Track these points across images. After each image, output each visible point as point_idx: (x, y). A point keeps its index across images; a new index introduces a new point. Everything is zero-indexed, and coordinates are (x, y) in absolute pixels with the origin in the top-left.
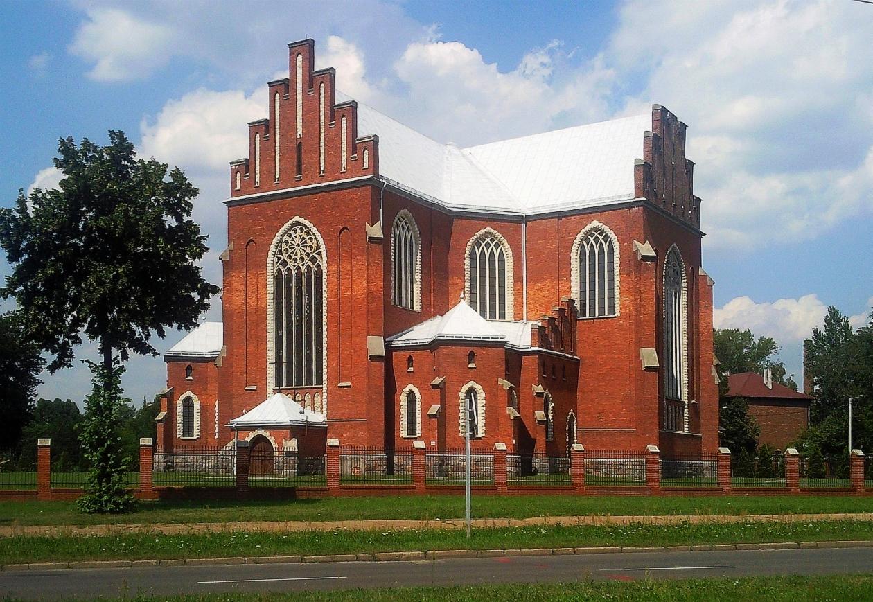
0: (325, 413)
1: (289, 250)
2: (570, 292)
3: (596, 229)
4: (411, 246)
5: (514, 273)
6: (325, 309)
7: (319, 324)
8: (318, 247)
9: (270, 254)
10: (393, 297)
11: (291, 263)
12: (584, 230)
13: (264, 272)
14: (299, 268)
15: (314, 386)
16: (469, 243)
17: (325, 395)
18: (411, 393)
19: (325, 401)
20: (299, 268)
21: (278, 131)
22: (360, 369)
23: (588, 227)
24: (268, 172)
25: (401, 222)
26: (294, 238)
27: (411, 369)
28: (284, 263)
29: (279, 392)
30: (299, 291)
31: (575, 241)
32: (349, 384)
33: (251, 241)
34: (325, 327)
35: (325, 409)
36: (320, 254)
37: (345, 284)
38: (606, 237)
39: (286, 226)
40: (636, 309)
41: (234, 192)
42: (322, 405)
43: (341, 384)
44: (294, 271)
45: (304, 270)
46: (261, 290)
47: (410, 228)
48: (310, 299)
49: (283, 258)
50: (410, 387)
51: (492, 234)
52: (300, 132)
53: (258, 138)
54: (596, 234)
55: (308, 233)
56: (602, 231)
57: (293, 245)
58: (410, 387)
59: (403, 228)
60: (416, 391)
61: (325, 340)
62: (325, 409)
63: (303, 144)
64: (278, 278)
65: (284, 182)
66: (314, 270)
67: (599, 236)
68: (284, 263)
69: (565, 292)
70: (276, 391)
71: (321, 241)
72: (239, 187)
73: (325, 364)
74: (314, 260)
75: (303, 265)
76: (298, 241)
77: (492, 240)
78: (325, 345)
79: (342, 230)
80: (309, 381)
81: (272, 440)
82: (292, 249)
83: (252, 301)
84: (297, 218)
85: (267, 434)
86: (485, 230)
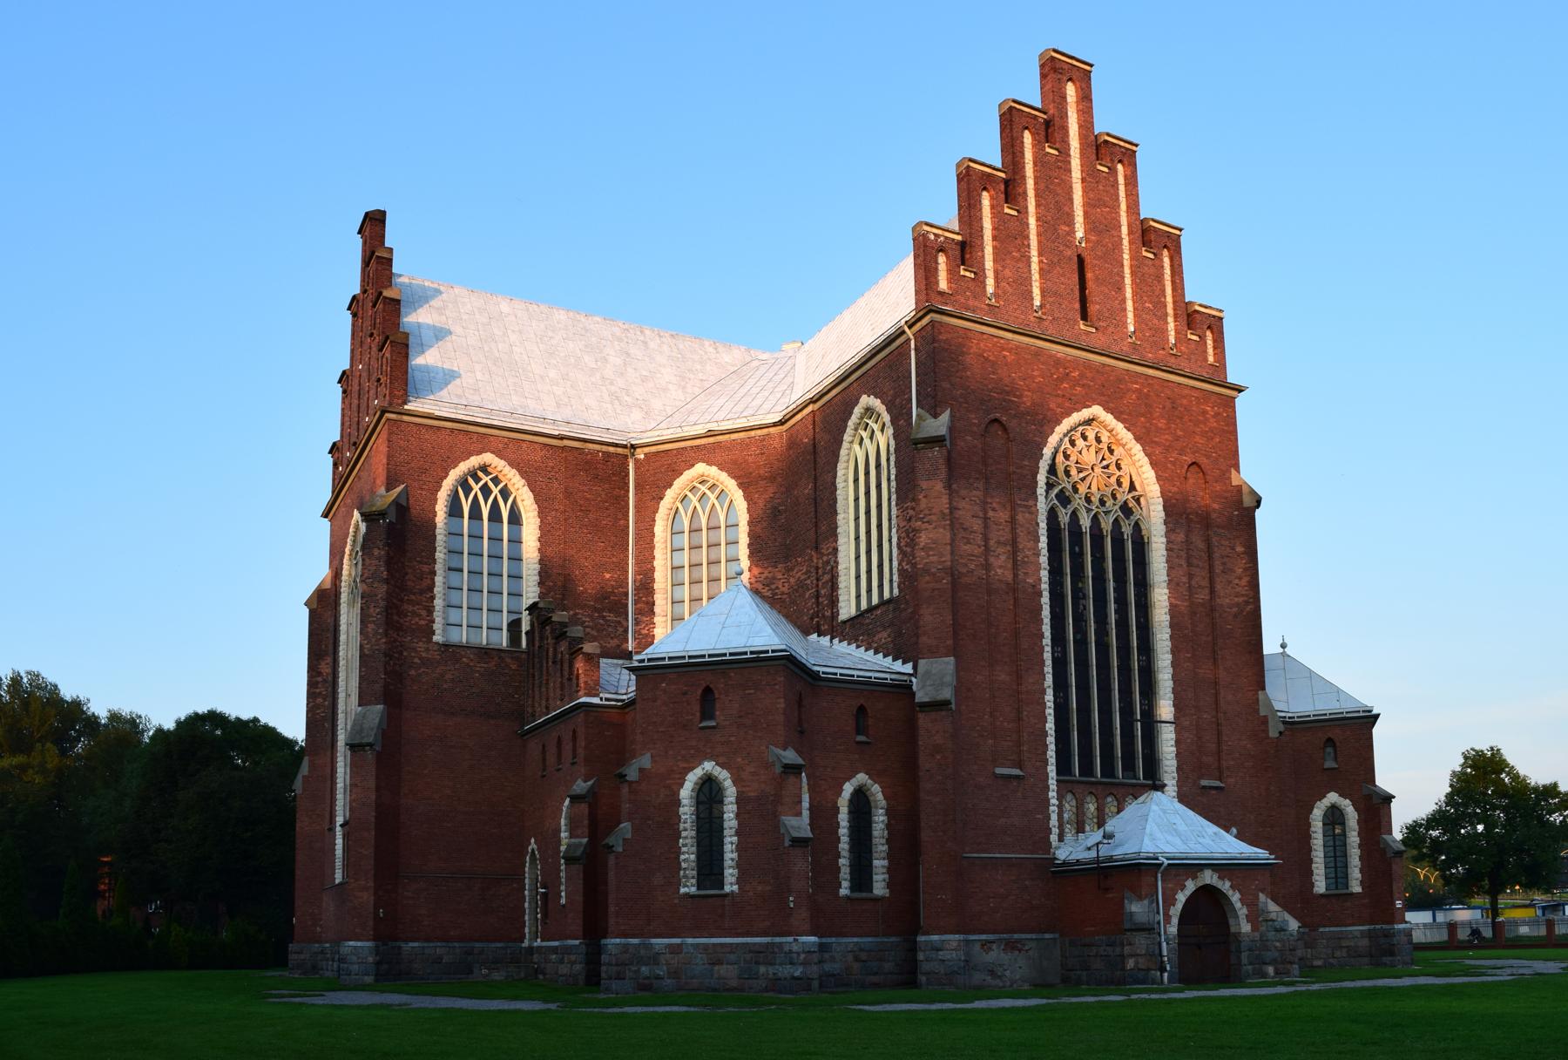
22: (1237, 755)
32: (1217, 783)
45: (1106, 525)
46: (1023, 542)
66: (1127, 530)
81: (1235, 898)
84: (1096, 410)
85: (1225, 886)
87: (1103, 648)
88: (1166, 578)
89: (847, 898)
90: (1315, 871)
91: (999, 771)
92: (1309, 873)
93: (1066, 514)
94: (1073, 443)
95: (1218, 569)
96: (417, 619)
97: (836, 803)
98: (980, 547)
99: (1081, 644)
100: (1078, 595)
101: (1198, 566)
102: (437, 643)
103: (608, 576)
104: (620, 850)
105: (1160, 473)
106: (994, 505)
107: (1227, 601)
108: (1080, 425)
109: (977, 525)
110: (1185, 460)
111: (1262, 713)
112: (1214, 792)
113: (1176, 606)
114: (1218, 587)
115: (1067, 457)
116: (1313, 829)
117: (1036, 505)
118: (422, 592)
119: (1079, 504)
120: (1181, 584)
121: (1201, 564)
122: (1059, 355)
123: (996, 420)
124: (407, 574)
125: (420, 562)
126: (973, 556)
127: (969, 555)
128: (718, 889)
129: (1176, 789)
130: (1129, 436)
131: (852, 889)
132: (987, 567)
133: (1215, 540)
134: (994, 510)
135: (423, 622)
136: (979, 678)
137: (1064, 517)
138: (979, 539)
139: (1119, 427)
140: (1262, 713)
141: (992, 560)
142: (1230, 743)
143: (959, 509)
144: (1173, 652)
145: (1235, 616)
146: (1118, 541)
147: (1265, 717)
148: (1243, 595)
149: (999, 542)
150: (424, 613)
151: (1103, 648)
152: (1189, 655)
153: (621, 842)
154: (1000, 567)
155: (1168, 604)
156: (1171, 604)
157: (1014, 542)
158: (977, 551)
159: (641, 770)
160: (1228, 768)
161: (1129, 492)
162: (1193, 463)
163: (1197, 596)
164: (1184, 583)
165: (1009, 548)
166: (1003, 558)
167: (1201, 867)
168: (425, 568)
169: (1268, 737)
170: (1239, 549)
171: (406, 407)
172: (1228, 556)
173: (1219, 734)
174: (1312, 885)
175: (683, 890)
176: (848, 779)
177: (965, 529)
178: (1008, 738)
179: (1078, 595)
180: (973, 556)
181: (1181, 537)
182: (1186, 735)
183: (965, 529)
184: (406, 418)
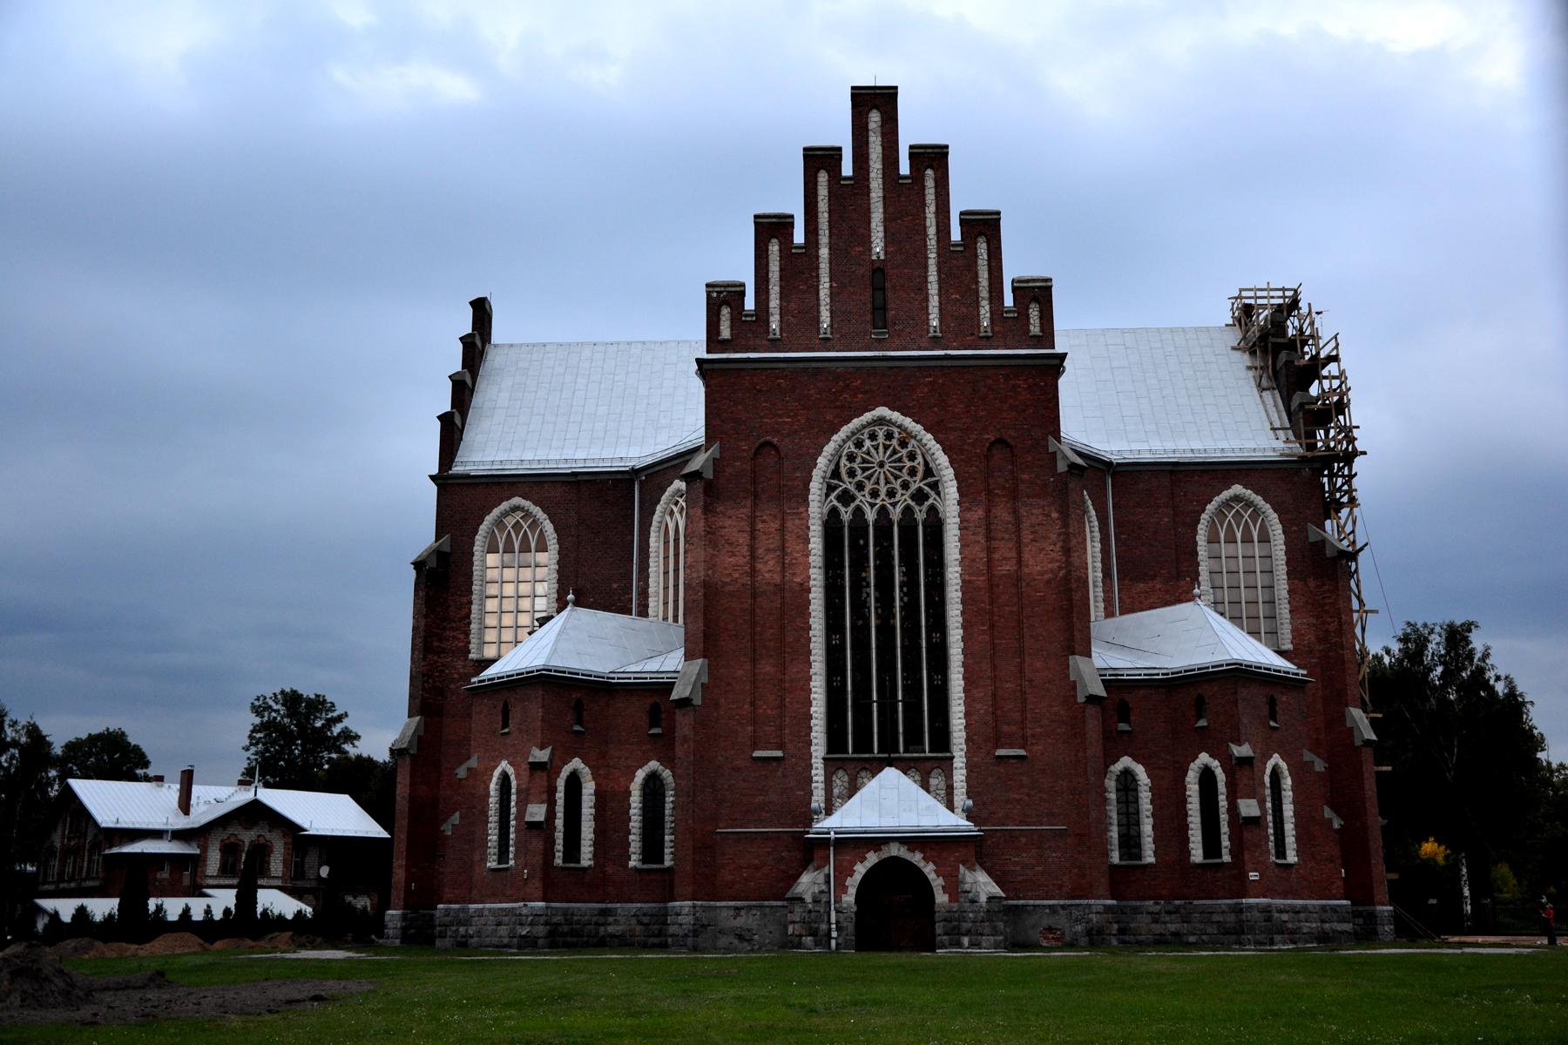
1: (859, 472)
3: (1237, 498)
11: (862, 499)
18: (1127, 774)
22: (1047, 722)
23: (1225, 495)
26: (872, 450)
28: (846, 498)
29: (891, 765)
31: (1203, 516)
32: (1022, 752)
37: (1005, 550)
40: (1320, 640)
41: (713, 341)
43: (1001, 752)
44: (871, 516)
45: (896, 514)
46: (793, 546)
52: (878, 247)
55: (903, 444)
56: (1249, 504)
58: (1126, 762)
60: (1140, 771)
64: (832, 525)
65: (840, 337)
66: (920, 515)
75: (894, 505)
79: (992, 444)
80: (914, 740)
81: (929, 870)
83: (768, 569)
85: (916, 858)
87: (886, 630)
88: (959, 557)
89: (636, 869)
90: (1192, 839)
91: (757, 754)
92: (1185, 840)
93: (846, 512)
94: (859, 444)
95: (1027, 537)
96: (457, 642)
97: (629, 787)
98: (745, 557)
100: (859, 584)
101: (1003, 539)
102: (472, 660)
103: (615, 586)
104: (450, 833)
105: (955, 456)
106: (765, 517)
107: (1039, 568)
109: (743, 539)
110: (987, 439)
111: (1072, 679)
112: (1012, 761)
113: (969, 582)
114: (1026, 556)
115: (851, 458)
116: (1188, 793)
117: (807, 511)
118: (461, 620)
119: (861, 501)
120: (978, 560)
121: (1007, 536)
122: (839, 370)
123: (768, 444)
124: (449, 606)
125: (460, 596)
126: (737, 566)
127: (733, 566)
128: (575, 863)
129: (965, 760)
130: (919, 427)
131: (644, 861)
132: (753, 572)
133: (1023, 511)
134: (764, 521)
135: (461, 644)
136: (740, 673)
137: (846, 514)
138: (745, 550)
139: (908, 422)
140: (1072, 679)
141: (759, 566)
142: (1037, 711)
143: (725, 527)
144: (964, 627)
145: (1049, 582)
147: (1075, 682)
148: (1057, 561)
149: (768, 550)
150: (462, 636)
151: (886, 630)
152: (985, 628)
153: (450, 827)
154: (769, 571)
155: (960, 581)
156: (963, 581)
157: (783, 548)
158: (742, 561)
159: (469, 769)
160: (1033, 736)
161: (924, 478)
162: (1000, 441)
163: (1000, 568)
164: (981, 559)
165: (778, 553)
166: (771, 563)
167: (887, 841)
168: (464, 600)
169: (1076, 703)
170: (1055, 515)
171: (450, 472)
172: (1039, 524)
173: (1024, 701)
174: (1189, 853)
175: (489, 864)
176: (641, 767)
177: (731, 544)
178: (772, 724)
179: (859, 584)
180: (737, 566)
181: (980, 513)
182: (979, 706)
183: (731, 544)
184: (450, 481)
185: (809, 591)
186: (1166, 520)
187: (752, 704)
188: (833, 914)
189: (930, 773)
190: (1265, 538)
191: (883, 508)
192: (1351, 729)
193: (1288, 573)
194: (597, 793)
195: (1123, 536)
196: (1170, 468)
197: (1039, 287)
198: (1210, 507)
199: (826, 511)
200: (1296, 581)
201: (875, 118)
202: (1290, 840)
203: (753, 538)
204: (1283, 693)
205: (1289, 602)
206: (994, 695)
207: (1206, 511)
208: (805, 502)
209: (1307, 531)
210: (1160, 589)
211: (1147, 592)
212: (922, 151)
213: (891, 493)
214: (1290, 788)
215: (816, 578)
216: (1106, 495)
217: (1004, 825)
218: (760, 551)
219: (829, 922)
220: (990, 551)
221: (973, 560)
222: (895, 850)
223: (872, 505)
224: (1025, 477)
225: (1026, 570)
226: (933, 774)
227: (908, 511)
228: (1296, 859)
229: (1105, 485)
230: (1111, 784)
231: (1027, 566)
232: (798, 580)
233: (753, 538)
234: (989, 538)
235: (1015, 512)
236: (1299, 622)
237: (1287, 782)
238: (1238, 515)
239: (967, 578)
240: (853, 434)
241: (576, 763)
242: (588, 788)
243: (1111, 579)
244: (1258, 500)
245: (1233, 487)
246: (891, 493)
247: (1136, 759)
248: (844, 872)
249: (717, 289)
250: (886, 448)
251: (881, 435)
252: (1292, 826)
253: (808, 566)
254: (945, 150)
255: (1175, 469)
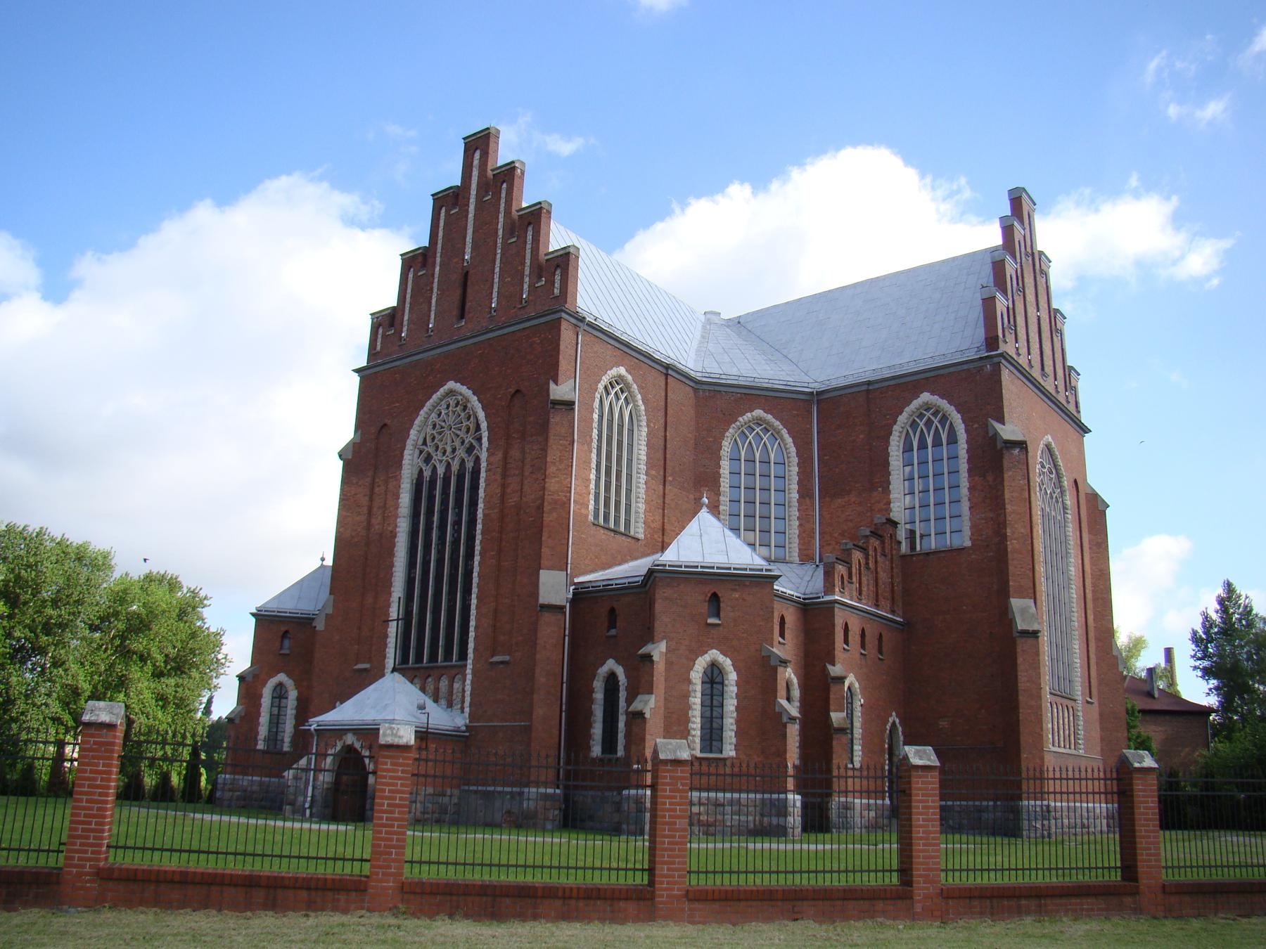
0: (467, 710)
2: (889, 510)
3: (927, 407)
4: (631, 431)
5: (799, 483)
6: (479, 527)
7: (470, 555)
8: (478, 428)
9: (410, 444)
10: (591, 507)
11: (437, 456)
12: (908, 410)
13: (398, 473)
14: (448, 466)
15: (454, 662)
16: (727, 434)
17: (469, 677)
18: (612, 677)
19: (468, 688)
20: (448, 466)
21: (438, 260)
23: (915, 404)
24: (420, 321)
25: (613, 387)
27: (613, 632)
28: (428, 459)
30: (445, 502)
31: (895, 427)
32: (507, 658)
33: (385, 425)
34: (477, 559)
35: (467, 704)
36: (479, 439)
38: (944, 419)
39: (435, 397)
42: (463, 696)
44: (441, 471)
45: (455, 467)
47: (630, 399)
48: (459, 515)
49: (426, 449)
50: (611, 664)
51: (768, 423)
53: (411, 276)
54: (928, 414)
57: (442, 427)
58: (611, 664)
59: (618, 398)
61: (475, 580)
62: (467, 704)
63: (471, 272)
67: (933, 418)
68: (428, 459)
69: (880, 511)
70: (394, 670)
71: (481, 415)
72: (379, 348)
73: (473, 623)
74: (470, 450)
75: (453, 459)
76: (452, 418)
77: (766, 430)
78: (475, 590)
82: (440, 433)
84: (451, 385)
86: (754, 413)
87: (440, 562)
91: (356, 667)
99: (426, 563)
107: (533, 497)
108: (441, 400)
112: (501, 666)
114: (526, 488)
138: (365, 510)
142: (520, 622)
146: (461, 477)
149: (379, 508)
151: (440, 562)
162: (518, 391)
181: (500, 455)
185: (395, 537)
186: (861, 436)
187: (359, 628)
188: (310, 789)
189: (454, 678)
190: (953, 440)
191: (447, 461)
192: (1011, 619)
193: (970, 471)
194: (299, 699)
195: (826, 458)
196: (864, 388)
197: (561, 256)
198: (903, 419)
199: (416, 473)
200: (977, 478)
201: (477, 155)
202: (730, 735)
203: (371, 500)
204: (735, 590)
205: (969, 500)
206: (496, 611)
207: (898, 423)
208: (400, 466)
209: (987, 426)
210: (854, 502)
211: (844, 506)
212: (498, 171)
213: (454, 450)
214: (734, 683)
215: (403, 527)
216: (811, 422)
217: (492, 721)
218: (375, 509)
219: (306, 796)
220: (504, 486)
221: (492, 497)
222: (350, 739)
223: (441, 461)
224: (532, 419)
225: (524, 499)
226: (456, 680)
227: (463, 462)
228: (733, 754)
229: (811, 413)
230: (598, 685)
231: (525, 497)
232: (390, 529)
233: (371, 500)
234: (504, 476)
235: (523, 452)
236: (978, 517)
237: (732, 676)
238: (929, 423)
239: (487, 512)
240: (435, 407)
241: (282, 677)
242: (293, 694)
243: (812, 497)
244: (944, 404)
245: (921, 395)
246: (454, 450)
247: (618, 662)
248: (321, 755)
249: (376, 316)
250: (454, 412)
251: (452, 403)
252: (732, 721)
253: (397, 517)
254: (513, 165)
255: (871, 388)
